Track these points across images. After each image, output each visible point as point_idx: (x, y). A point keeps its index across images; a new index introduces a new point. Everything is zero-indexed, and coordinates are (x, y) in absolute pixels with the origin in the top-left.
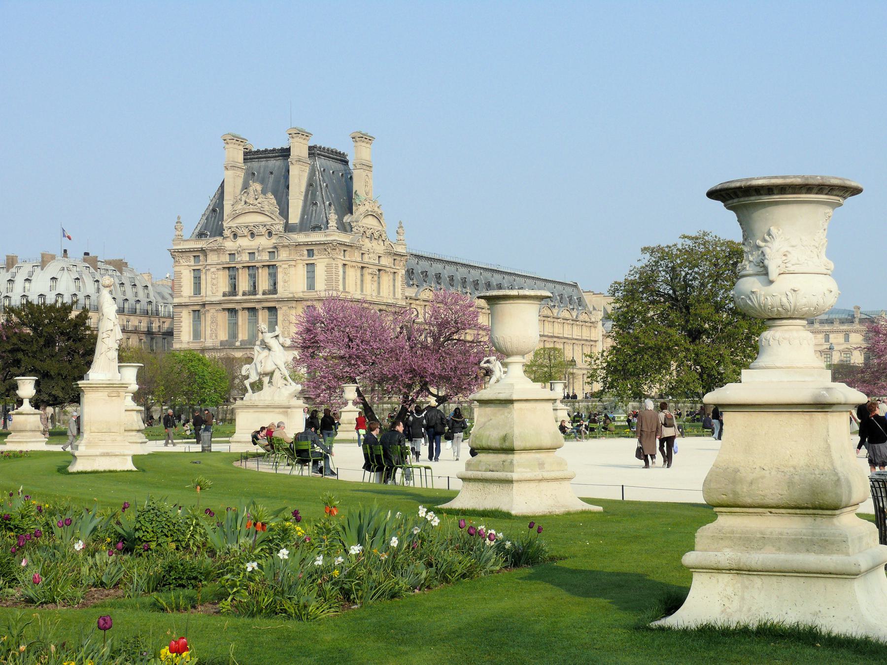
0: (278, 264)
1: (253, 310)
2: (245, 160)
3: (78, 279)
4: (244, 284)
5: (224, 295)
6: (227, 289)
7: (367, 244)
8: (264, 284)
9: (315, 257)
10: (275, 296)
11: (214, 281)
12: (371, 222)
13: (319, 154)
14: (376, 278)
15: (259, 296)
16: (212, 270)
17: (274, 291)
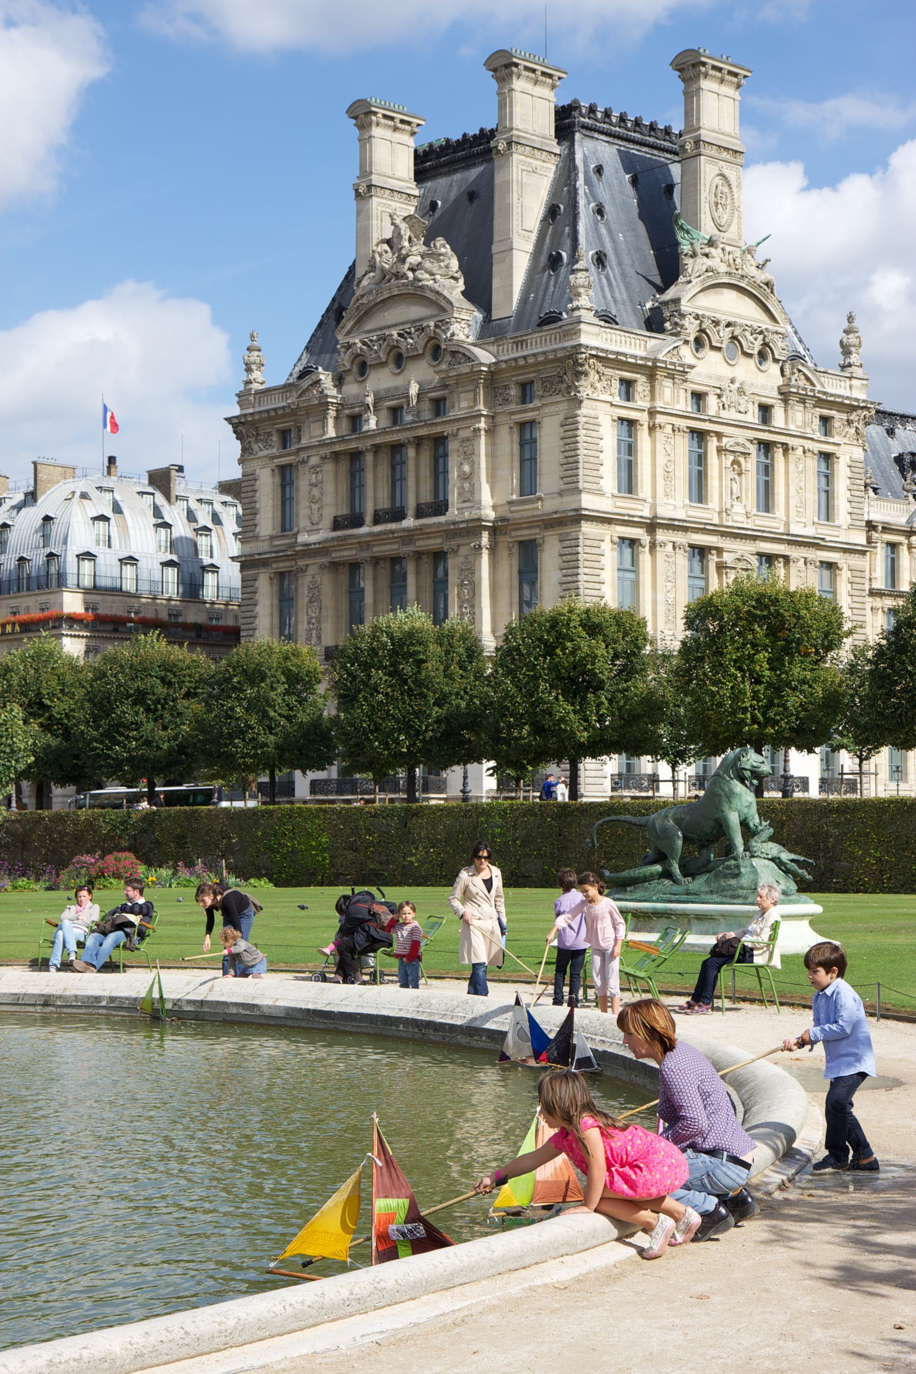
0: (448, 430)
1: (396, 560)
2: (420, 176)
3: (103, 518)
4: (376, 496)
5: (337, 525)
6: (344, 511)
7: (709, 368)
8: (417, 490)
9: (537, 403)
10: (442, 519)
11: (316, 492)
12: (731, 306)
13: (585, 127)
14: (751, 465)
15: (409, 522)
16: (314, 461)
17: (440, 507)
